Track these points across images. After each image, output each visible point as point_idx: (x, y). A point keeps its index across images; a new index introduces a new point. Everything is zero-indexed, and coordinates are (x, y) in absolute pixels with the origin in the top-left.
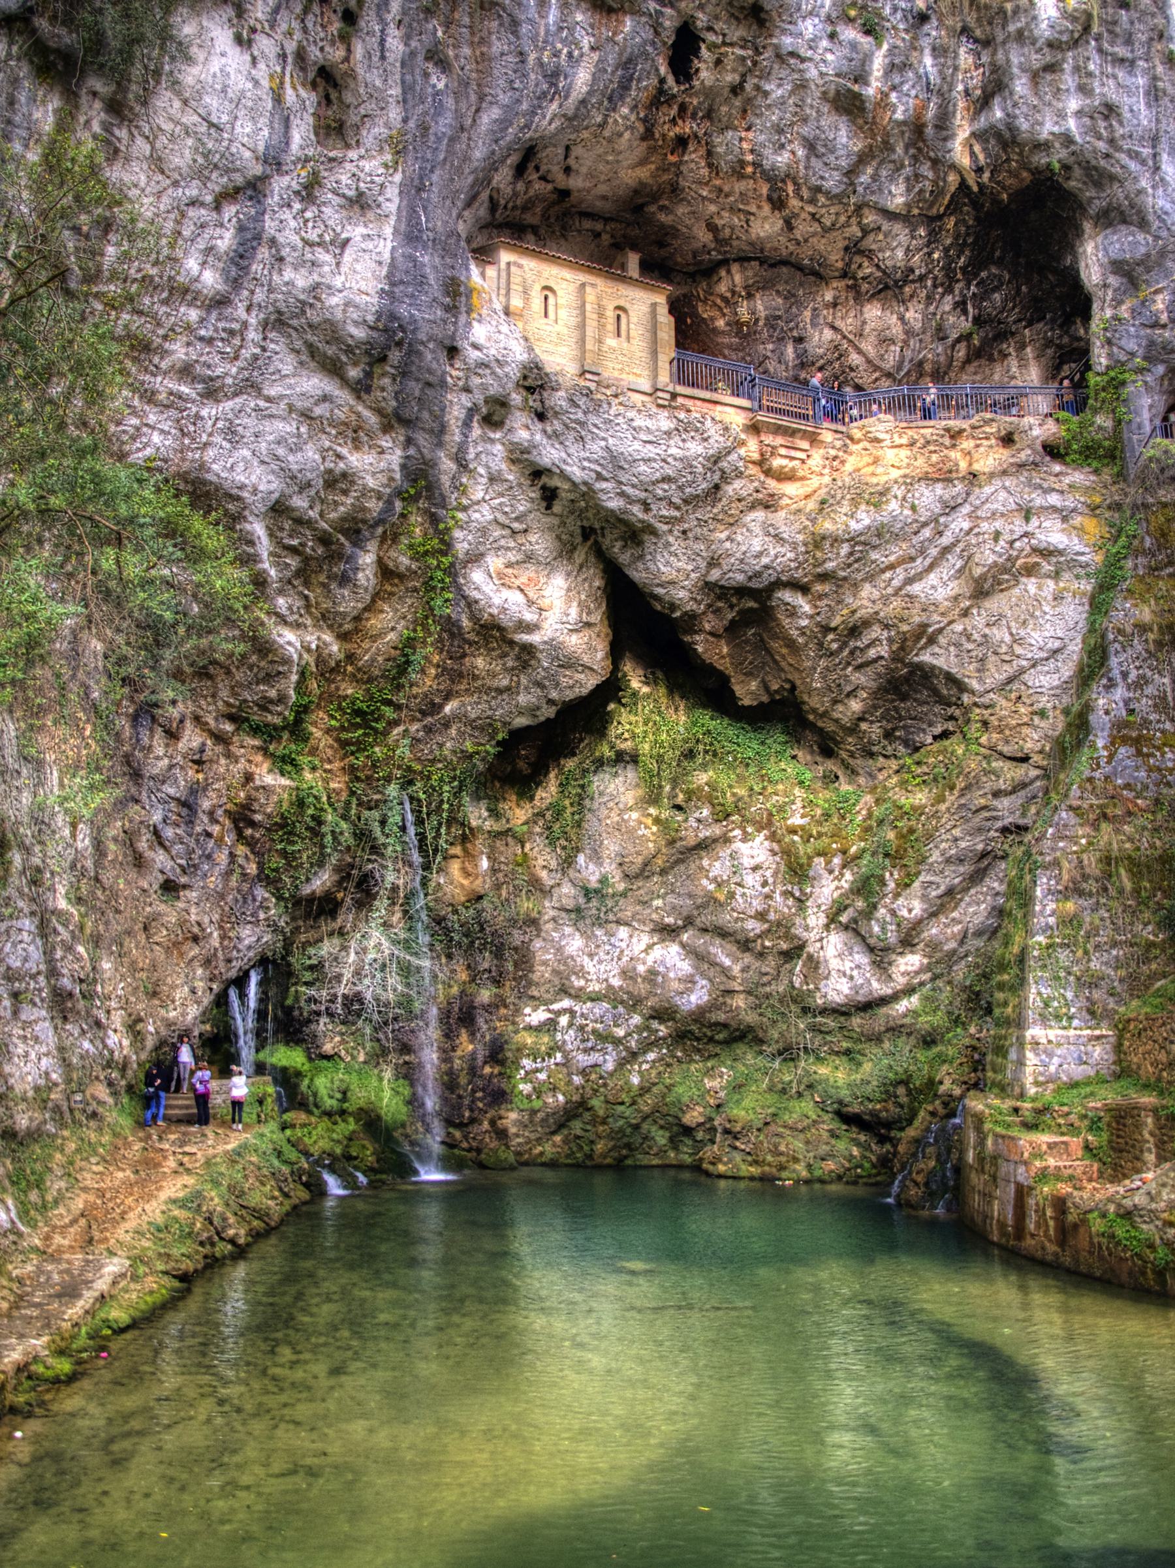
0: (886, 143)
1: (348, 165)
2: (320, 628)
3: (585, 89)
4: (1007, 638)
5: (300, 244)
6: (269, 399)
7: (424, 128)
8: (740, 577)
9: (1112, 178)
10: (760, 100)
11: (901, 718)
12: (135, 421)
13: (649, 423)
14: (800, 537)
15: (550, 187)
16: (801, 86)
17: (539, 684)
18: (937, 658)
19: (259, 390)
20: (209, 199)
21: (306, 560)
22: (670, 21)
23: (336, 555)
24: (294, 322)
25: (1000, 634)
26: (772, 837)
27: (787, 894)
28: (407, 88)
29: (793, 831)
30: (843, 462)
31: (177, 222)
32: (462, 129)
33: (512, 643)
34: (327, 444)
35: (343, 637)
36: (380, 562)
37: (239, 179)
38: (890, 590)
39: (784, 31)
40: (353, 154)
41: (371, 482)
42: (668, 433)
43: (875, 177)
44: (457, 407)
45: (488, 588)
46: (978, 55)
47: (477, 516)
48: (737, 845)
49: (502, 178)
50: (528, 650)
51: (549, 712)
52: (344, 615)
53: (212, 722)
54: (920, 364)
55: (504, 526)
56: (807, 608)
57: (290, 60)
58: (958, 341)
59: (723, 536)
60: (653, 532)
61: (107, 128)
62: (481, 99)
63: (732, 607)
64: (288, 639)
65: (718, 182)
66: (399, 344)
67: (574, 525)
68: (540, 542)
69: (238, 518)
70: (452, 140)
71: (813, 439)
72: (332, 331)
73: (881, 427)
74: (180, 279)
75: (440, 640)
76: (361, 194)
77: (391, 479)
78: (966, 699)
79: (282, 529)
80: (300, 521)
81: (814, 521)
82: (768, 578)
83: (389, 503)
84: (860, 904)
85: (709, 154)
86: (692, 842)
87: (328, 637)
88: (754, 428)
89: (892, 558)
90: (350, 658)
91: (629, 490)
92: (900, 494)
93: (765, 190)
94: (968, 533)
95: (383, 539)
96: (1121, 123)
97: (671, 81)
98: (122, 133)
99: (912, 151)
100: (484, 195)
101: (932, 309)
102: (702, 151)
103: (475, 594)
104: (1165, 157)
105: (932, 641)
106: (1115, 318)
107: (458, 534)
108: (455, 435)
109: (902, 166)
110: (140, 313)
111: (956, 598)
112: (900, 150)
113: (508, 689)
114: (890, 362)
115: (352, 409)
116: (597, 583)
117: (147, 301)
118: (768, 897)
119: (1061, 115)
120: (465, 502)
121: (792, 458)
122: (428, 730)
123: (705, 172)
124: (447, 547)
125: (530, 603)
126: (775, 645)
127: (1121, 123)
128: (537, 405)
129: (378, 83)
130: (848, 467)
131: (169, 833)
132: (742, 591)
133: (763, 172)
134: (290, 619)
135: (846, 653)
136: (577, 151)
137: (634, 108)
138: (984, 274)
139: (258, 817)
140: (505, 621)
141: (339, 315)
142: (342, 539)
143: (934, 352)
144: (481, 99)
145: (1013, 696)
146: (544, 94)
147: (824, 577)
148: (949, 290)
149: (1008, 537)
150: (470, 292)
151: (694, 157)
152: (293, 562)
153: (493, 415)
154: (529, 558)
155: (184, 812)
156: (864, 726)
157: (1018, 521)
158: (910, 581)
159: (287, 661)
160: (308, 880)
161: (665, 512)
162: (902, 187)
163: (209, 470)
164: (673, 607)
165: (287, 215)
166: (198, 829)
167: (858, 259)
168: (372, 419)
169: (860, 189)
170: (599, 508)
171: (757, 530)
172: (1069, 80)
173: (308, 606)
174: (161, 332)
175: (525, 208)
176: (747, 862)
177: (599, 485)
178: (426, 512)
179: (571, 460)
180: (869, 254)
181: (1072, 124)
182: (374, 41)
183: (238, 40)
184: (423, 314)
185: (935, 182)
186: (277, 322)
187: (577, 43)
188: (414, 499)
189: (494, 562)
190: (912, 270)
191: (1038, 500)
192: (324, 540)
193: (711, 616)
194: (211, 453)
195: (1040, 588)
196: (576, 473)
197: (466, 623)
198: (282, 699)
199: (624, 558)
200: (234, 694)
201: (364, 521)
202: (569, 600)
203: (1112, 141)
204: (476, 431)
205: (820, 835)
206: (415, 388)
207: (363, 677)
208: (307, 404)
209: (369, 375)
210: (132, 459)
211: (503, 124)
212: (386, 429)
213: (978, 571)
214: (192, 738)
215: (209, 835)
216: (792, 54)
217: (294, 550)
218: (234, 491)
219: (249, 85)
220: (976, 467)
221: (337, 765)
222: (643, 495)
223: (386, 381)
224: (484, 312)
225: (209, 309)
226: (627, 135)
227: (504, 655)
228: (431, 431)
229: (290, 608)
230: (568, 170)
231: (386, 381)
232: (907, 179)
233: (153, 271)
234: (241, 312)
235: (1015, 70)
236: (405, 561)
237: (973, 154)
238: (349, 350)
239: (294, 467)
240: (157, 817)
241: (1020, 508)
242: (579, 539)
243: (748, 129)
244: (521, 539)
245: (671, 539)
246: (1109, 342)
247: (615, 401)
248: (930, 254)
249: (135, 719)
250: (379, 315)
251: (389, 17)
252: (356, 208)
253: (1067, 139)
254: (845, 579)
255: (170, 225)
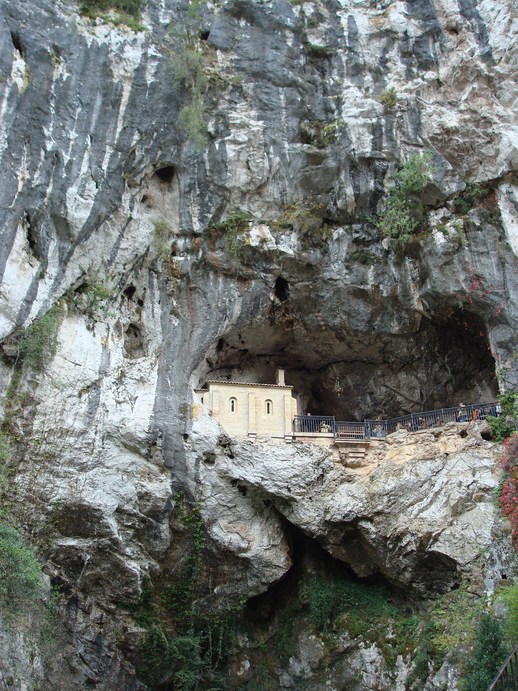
0: (382, 306)
1: (137, 366)
2: (149, 559)
3: (239, 312)
4: (473, 535)
5: (115, 403)
6: (108, 468)
7: (169, 344)
8: (339, 517)
9: (488, 305)
10: (320, 300)
11: (433, 580)
12: (51, 485)
13: (283, 452)
14: (364, 496)
15: (237, 350)
16: (338, 291)
17: (256, 576)
18: (440, 548)
19: (103, 465)
20: (76, 393)
21: (137, 530)
22: (271, 278)
23: (150, 527)
24: (115, 435)
25: (469, 533)
26: (379, 646)
27: (387, 676)
28: (163, 327)
29: (388, 641)
30: (384, 455)
31: (63, 405)
32: (185, 341)
33: (238, 558)
34: (137, 482)
35: (161, 562)
36: (171, 527)
37: (89, 383)
38: (412, 516)
39: (324, 271)
40: (140, 360)
41: (159, 495)
42: (293, 455)
43: (382, 321)
44: (191, 458)
45: (221, 534)
46: (414, 263)
47: (209, 503)
48: (363, 651)
49: (211, 353)
50: (246, 560)
51: (265, 589)
52: (158, 552)
53: (105, 605)
54: (432, 396)
55: (224, 506)
56: (373, 529)
57: (112, 329)
58: (447, 383)
59: (329, 498)
60: (294, 500)
61: (33, 377)
62: (193, 326)
63: (342, 531)
64: (134, 566)
65: (312, 335)
66: (161, 437)
67: (260, 500)
68: (244, 510)
69: (101, 518)
70: (181, 346)
71: (367, 446)
72: (130, 436)
73: (401, 436)
74: (65, 427)
75: (204, 559)
76: (142, 377)
77: (167, 493)
78: (458, 568)
79: (123, 519)
80: (130, 515)
81: (368, 487)
82: (352, 516)
83: (169, 502)
84: (418, 680)
85: (305, 324)
86: (341, 650)
87: (153, 563)
88: (336, 446)
89: (411, 500)
90: (166, 571)
91: (279, 483)
92: (409, 468)
93: (333, 334)
94: (447, 483)
95: (170, 518)
96: (486, 281)
97: (277, 301)
98: (39, 377)
99: (396, 308)
100: (204, 363)
101: (429, 371)
102: (301, 324)
103: (216, 538)
104: (511, 292)
105: (436, 540)
106: (504, 368)
107: (202, 512)
108: (192, 470)
109: (393, 315)
110: (49, 443)
111: (445, 517)
112: (390, 308)
113: (242, 579)
114: (417, 397)
115: (146, 466)
116: (277, 525)
117: (52, 438)
118: (378, 677)
119: (457, 282)
120: (203, 498)
121: (357, 457)
122: (208, 601)
123: (305, 332)
124: (199, 518)
125: (243, 539)
126: (366, 547)
127: (486, 281)
128: (228, 452)
129: (153, 327)
130: (387, 457)
131: (88, 657)
132: (342, 523)
133: (331, 328)
134: (133, 557)
135: (397, 549)
136: (243, 335)
137: (263, 315)
138: (450, 352)
139: (132, 647)
140: (232, 548)
141: (132, 430)
142: (151, 520)
143: (435, 390)
144: (193, 326)
145: (481, 564)
146: (221, 319)
147: (378, 513)
148: (435, 361)
149: (465, 484)
150: (191, 410)
151: (297, 327)
152: (131, 532)
153: (209, 459)
154: (239, 518)
155: (95, 647)
156: (414, 585)
157: (470, 475)
158: (421, 511)
159: (135, 575)
160: (162, 676)
161: (298, 491)
162: (396, 323)
163: (84, 501)
164: (312, 534)
165: (110, 393)
166: (103, 654)
167: (387, 355)
168: (155, 468)
169: (376, 327)
170: (268, 493)
171: (344, 494)
172: (458, 267)
173: (142, 550)
174: (59, 449)
175: (228, 360)
176: (368, 659)
177: (263, 483)
178: (187, 504)
179: (250, 475)
180: (391, 352)
181: (463, 285)
182: (150, 310)
183: (88, 328)
184: (171, 423)
185: (410, 319)
186: (108, 436)
187: (233, 296)
188: (182, 497)
189: (223, 522)
190: (414, 356)
191: (478, 465)
192: (143, 521)
193: (332, 536)
194: (84, 494)
195: (486, 508)
196: (252, 479)
197: (215, 551)
198: (136, 592)
199: (286, 513)
200: (113, 592)
201: (159, 512)
202: (263, 535)
203: (483, 290)
204: (202, 467)
205: (401, 643)
206: (171, 454)
207: (173, 578)
208: (125, 467)
209: (150, 451)
210: (51, 501)
211: (204, 335)
212: (162, 471)
213: (452, 503)
214: (96, 613)
215: (109, 657)
216: (331, 279)
217: (130, 527)
218: (97, 508)
219: (92, 345)
220: (448, 450)
221: (169, 620)
222: (286, 484)
223: (158, 453)
224: (199, 417)
225: (78, 436)
226: (263, 325)
227: (237, 563)
228: (182, 470)
229: (132, 552)
230: (243, 342)
231: (158, 453)
232: (397, 319)
233: (53, 426)
234: (93, 435)
235: (432, 267)
236: (181, 526)
237: (423, 304)
238: (140, 443)
239: (122, 494)
240: (81, 650)
241: (470, 469)
242: (264, 506)
243: (319, 312)
244: (234, 510)
245: (304, 502)
246: (504, 380)
247: (265, 445)
248: (420, 348)
249: (68, 607)
250: (150, 427)
251: (155, 300)
252: (141, 383)
253: (462, 292)
254: (389, 513)
255: (60, 407)
